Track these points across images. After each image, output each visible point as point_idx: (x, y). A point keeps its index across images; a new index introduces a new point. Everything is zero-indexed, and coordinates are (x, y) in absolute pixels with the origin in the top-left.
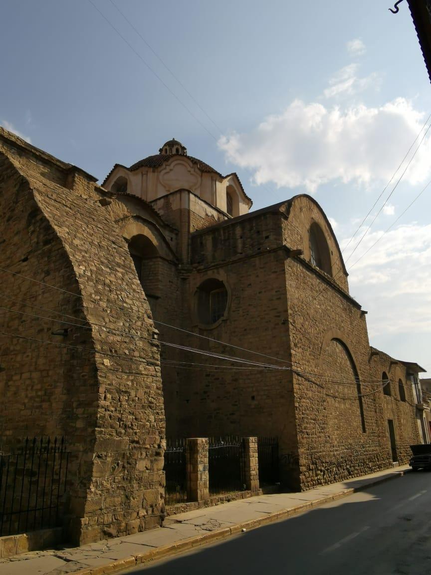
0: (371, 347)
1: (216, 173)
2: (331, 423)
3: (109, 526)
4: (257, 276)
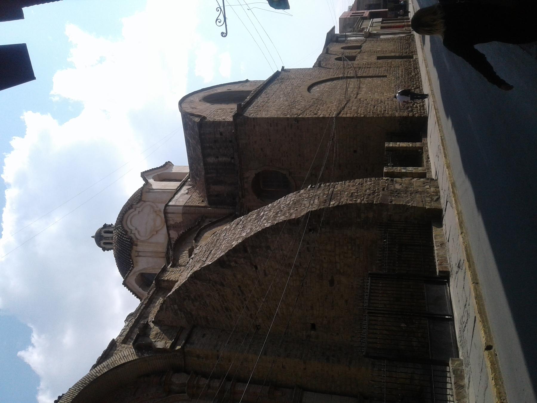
0: (313, 67)
1: (142, 188)
2: (376, 96)
3: (432, 200)
4: (255, 142)
